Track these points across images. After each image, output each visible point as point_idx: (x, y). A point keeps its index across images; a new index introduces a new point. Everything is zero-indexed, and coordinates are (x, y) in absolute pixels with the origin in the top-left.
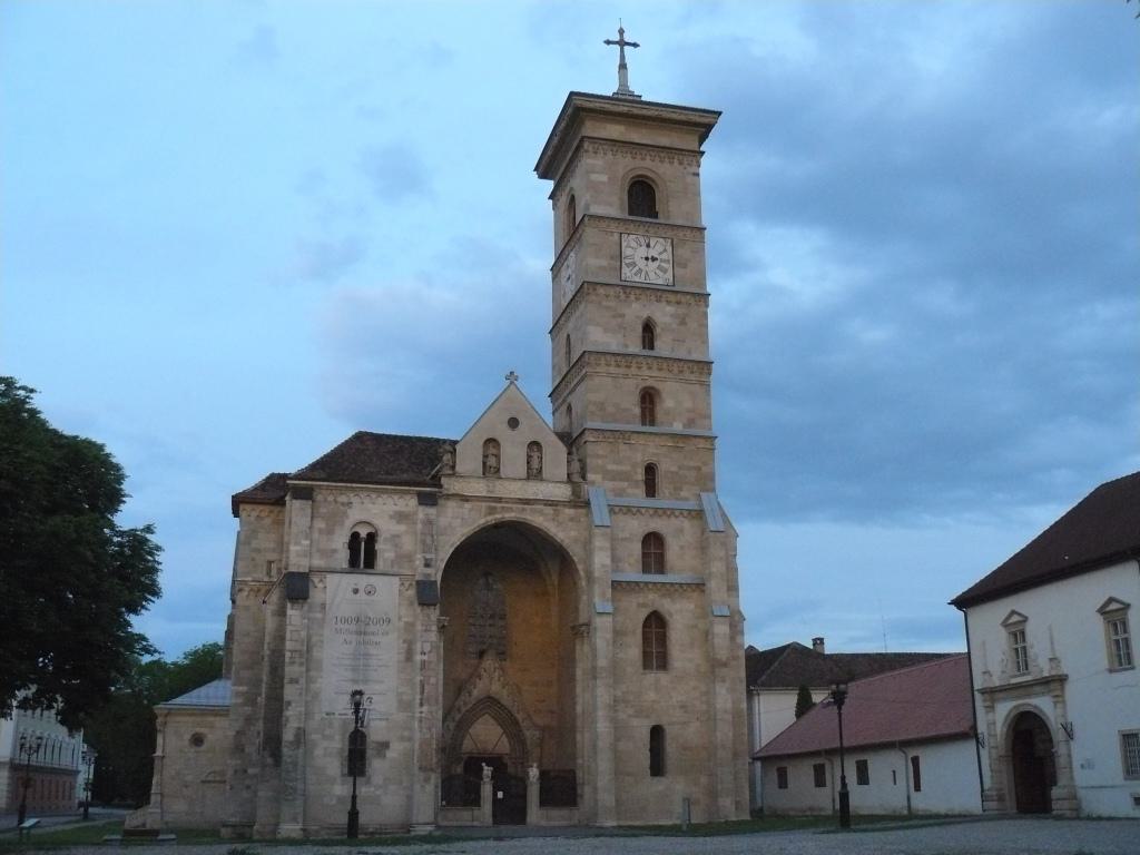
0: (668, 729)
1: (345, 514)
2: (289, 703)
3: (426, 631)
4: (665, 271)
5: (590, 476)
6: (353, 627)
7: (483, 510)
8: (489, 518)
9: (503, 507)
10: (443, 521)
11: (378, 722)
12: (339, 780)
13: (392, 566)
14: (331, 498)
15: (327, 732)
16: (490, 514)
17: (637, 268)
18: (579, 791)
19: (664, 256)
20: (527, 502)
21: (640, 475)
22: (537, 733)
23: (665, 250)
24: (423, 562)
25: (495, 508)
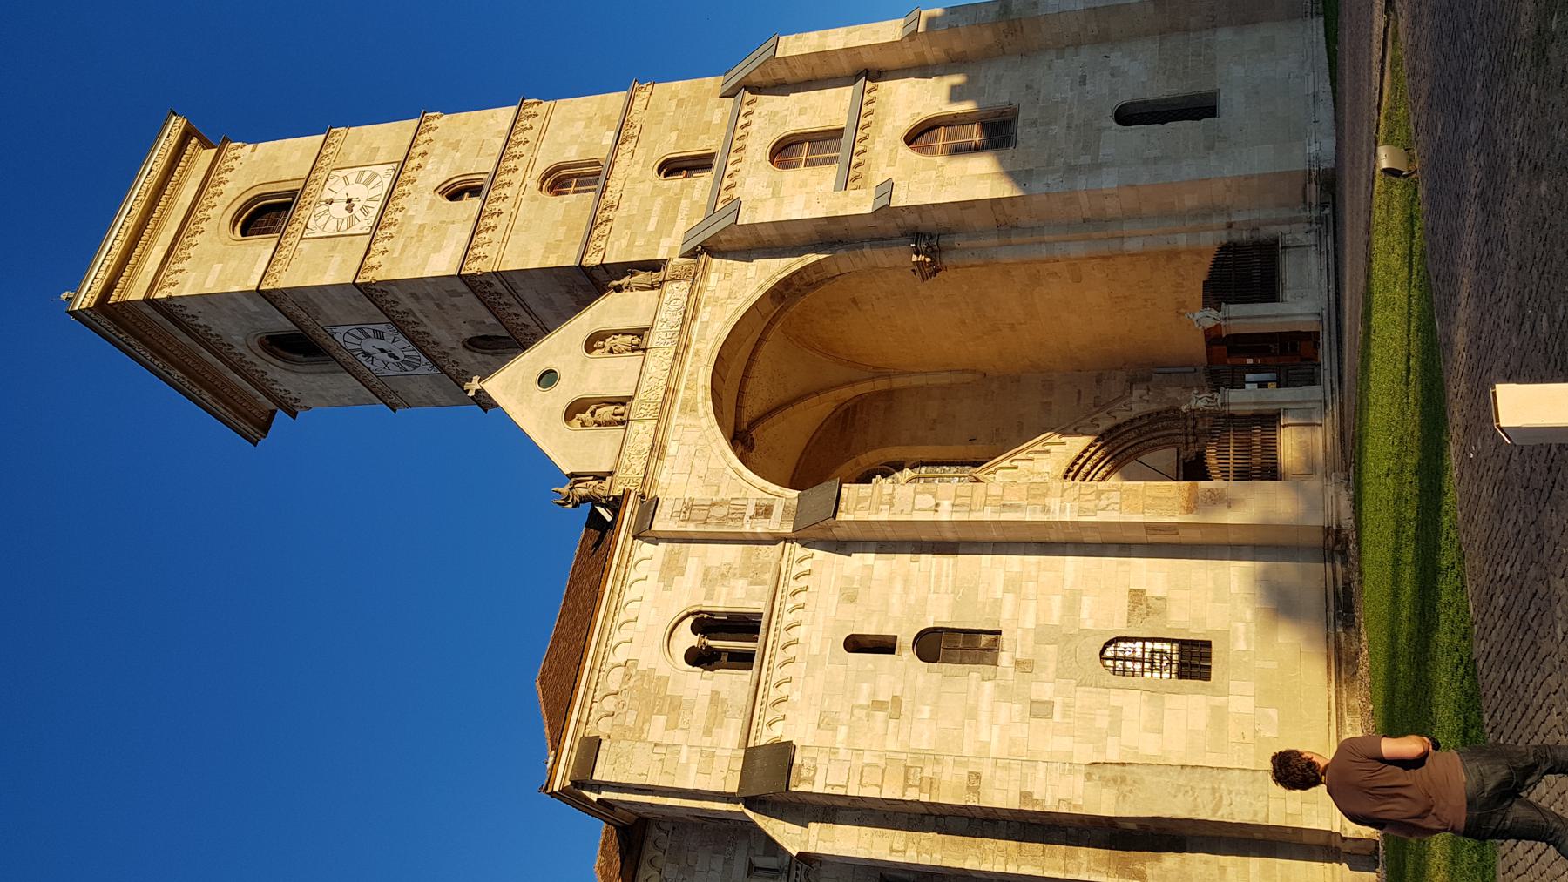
0: (1127, 99)
2: (1026, 796)
3: (892, 505)
4: (375, 175)
5: (660, 255)
7: (679, 421)
8: (701, 411)
9: (686, 388)
11: (1084, 614)
12: (1218, 700)
13: (764, 583)
14: (609, 704)
15: (1103, 722)
16: (694, 410)
17: (360, 215)
18: (1245, 235)
19: (352, 179)
21: (676, 182)
22: (1136, 393)
23: (345, 178)
24: (761, 520)
25: (685, 402)
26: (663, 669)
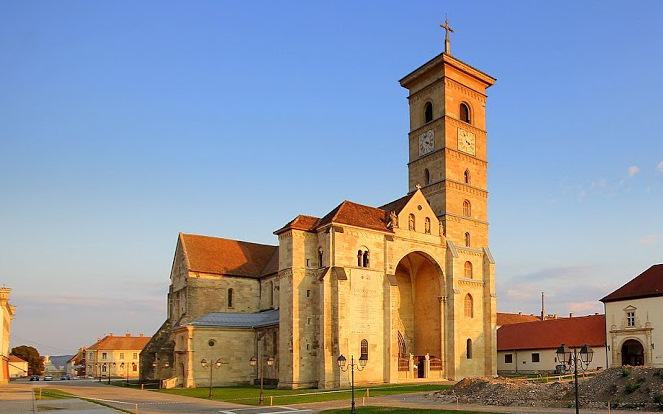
1: (356, 242)
6: (362, 294)
10: (395, 248)
20: (426, 243)
26: (358, 245)
